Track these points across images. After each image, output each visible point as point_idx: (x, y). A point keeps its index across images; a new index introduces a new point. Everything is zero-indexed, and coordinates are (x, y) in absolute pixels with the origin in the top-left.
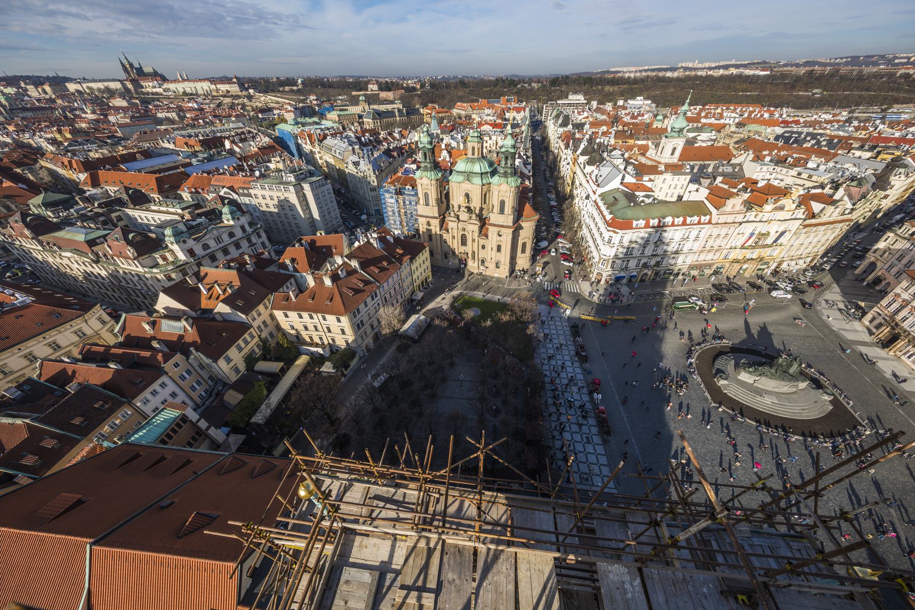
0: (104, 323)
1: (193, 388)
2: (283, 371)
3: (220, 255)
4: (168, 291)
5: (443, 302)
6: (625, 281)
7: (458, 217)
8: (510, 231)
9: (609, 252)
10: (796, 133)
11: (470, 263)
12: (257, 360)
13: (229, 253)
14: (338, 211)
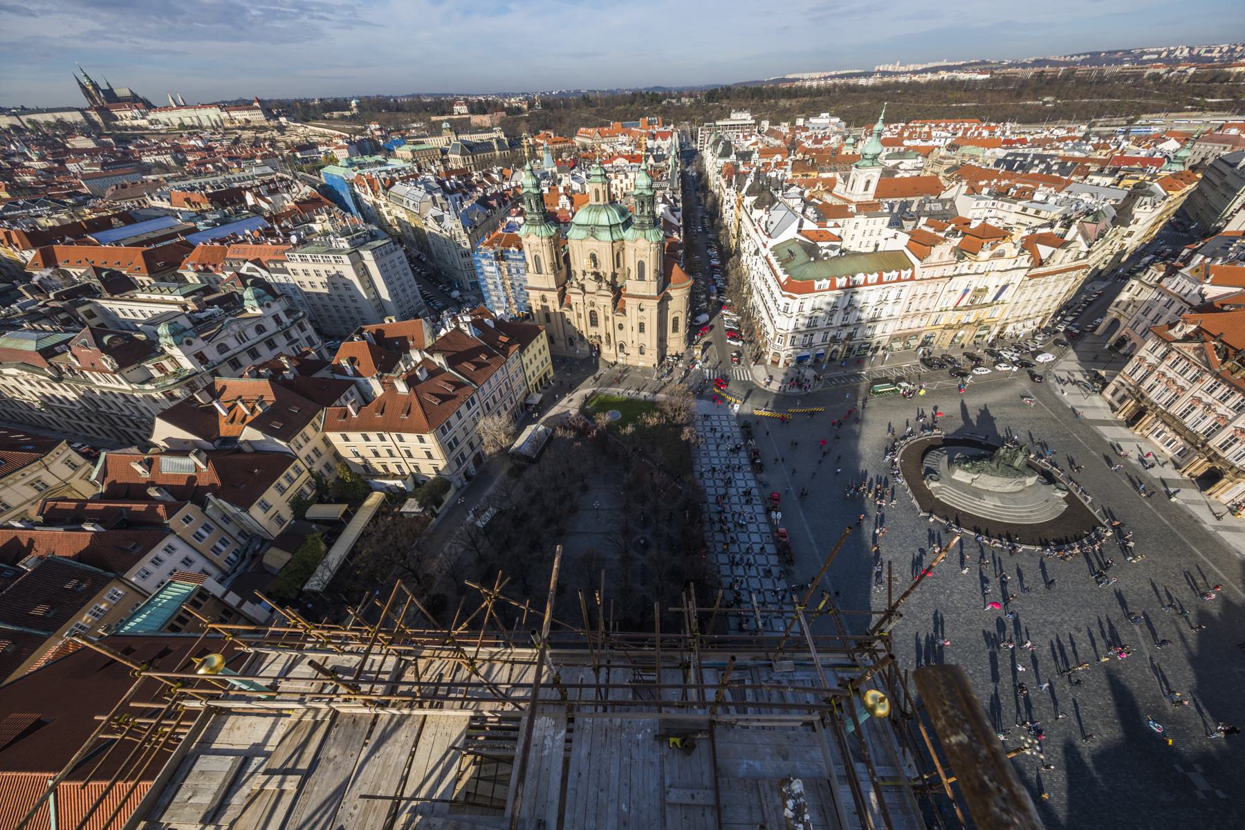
0: (75, 467)
1: (216, 550)
2: (348, 516)
3: (245, 359)
4: (168, 416)
5: (570, 405)
6: (809, 361)
7: (583, 287)
8: (655, 303)
9: (786, 324)
10: (1020, 155)
11: (605, 350)
12: (309, 504)
13: (259, 356)
14: (416, 287)
